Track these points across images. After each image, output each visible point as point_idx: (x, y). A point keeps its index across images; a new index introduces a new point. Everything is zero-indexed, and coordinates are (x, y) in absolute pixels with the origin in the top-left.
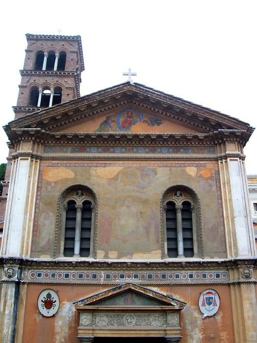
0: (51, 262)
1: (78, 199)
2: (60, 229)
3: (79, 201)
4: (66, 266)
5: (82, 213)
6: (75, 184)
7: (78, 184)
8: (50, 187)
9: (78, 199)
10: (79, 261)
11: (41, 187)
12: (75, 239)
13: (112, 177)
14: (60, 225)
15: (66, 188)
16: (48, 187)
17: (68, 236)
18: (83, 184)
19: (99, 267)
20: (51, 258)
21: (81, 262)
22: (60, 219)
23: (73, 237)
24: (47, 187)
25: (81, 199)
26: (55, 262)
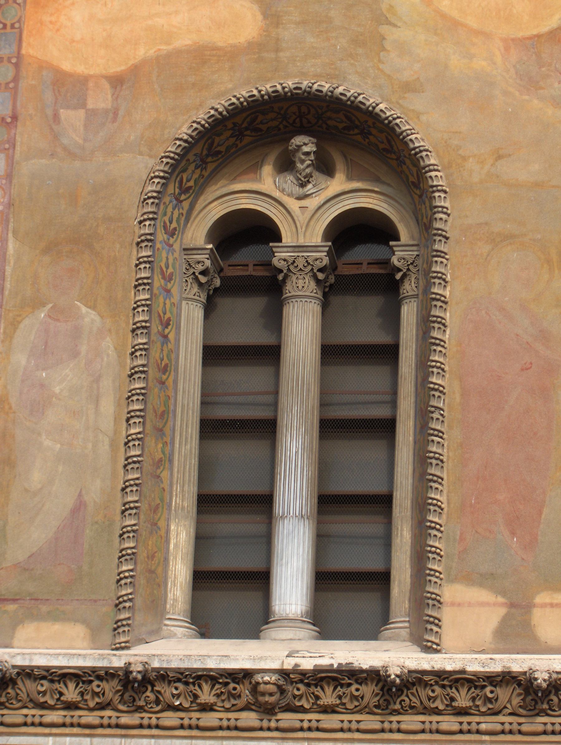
0: (94, 670)
1: (294, 205)
2: (160, 431)
3: (302, 218)
4: (207, 708)
5: (325, 306)
6: (267, 87)
7: (290, 84)
8: (81, 113)
9: (294, 205)
10: (307, 664)
11: (15, 118)
12: (279, 508)
13: (544, 29)
14: (155, 398)
15: (202, 116)
16: (63, 113)
17: (209, 490)
18: (326, 87)
19: (462, 712)
20: (95, 644)
21: (317, 670)
22: (155, 353)
23: (260, 489)
24: (56, 117)
25: (312, 203)
26: (127, 669)
